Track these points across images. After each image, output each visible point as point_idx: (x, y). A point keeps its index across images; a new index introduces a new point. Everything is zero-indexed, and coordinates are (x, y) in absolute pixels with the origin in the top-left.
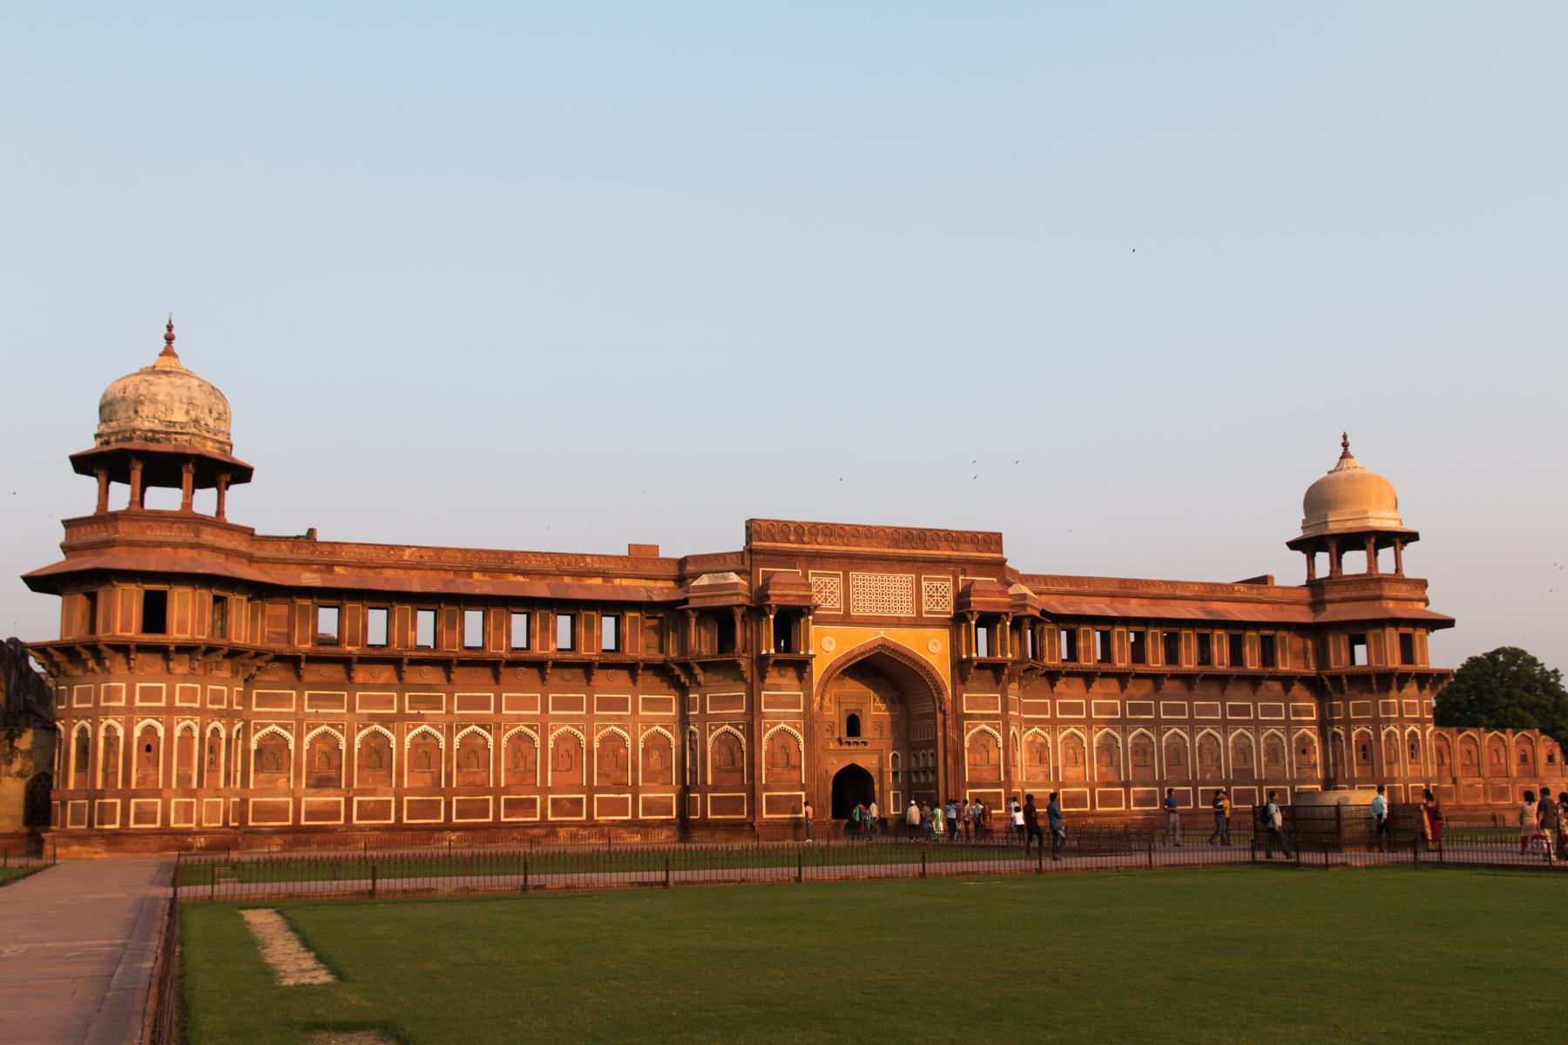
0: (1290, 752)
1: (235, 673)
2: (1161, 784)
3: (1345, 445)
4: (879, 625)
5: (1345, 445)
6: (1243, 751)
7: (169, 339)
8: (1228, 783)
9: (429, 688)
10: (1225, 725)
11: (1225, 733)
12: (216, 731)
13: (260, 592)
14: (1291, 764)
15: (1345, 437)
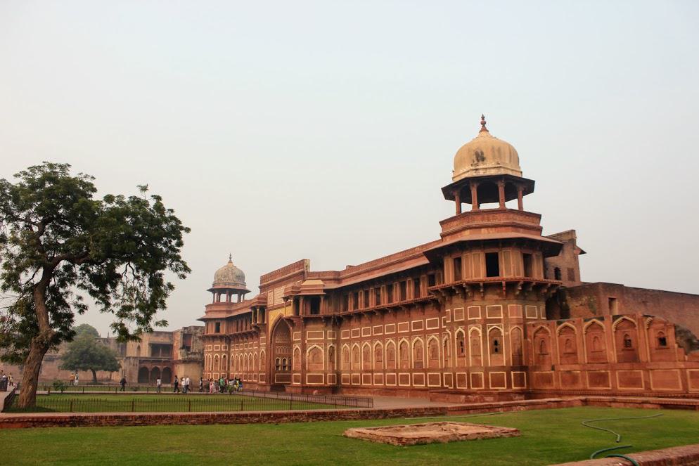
0: (441, 350)
1: (221, 341)
2: (384, 371)
3: (483, 124)
4: (279, 308)
5: (483, 124)
6: (419, 351)
7: (230, 258)
8: (411, 371)
9: (246, 342)
10: (410, 335)
11: (410, 340)
12: (217, 356)
13: (229, 320)
14: (441, 357)
15: (483, 118)
